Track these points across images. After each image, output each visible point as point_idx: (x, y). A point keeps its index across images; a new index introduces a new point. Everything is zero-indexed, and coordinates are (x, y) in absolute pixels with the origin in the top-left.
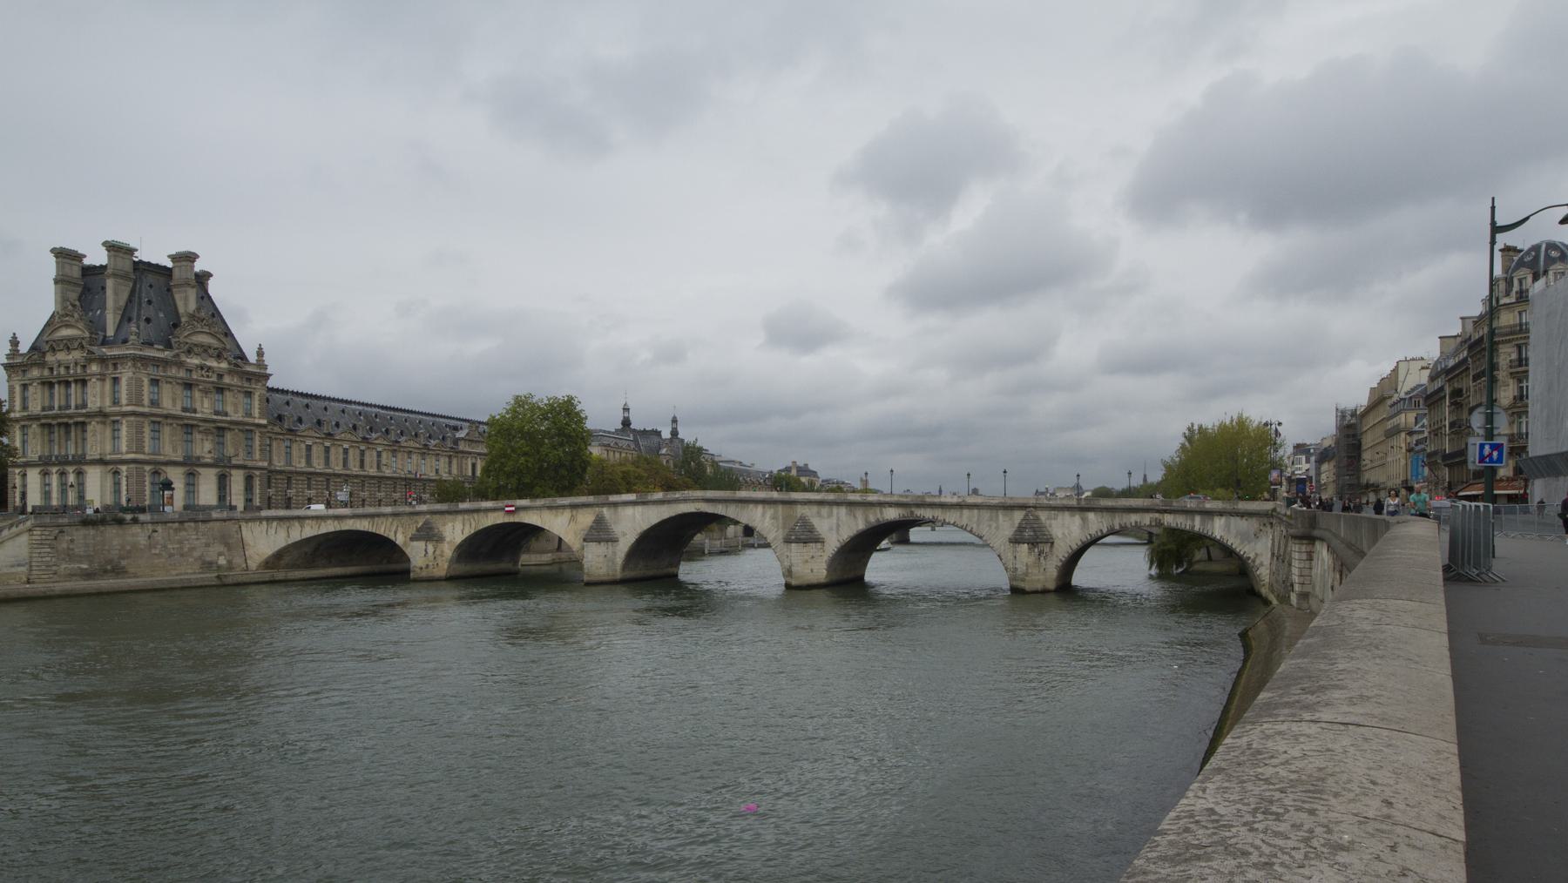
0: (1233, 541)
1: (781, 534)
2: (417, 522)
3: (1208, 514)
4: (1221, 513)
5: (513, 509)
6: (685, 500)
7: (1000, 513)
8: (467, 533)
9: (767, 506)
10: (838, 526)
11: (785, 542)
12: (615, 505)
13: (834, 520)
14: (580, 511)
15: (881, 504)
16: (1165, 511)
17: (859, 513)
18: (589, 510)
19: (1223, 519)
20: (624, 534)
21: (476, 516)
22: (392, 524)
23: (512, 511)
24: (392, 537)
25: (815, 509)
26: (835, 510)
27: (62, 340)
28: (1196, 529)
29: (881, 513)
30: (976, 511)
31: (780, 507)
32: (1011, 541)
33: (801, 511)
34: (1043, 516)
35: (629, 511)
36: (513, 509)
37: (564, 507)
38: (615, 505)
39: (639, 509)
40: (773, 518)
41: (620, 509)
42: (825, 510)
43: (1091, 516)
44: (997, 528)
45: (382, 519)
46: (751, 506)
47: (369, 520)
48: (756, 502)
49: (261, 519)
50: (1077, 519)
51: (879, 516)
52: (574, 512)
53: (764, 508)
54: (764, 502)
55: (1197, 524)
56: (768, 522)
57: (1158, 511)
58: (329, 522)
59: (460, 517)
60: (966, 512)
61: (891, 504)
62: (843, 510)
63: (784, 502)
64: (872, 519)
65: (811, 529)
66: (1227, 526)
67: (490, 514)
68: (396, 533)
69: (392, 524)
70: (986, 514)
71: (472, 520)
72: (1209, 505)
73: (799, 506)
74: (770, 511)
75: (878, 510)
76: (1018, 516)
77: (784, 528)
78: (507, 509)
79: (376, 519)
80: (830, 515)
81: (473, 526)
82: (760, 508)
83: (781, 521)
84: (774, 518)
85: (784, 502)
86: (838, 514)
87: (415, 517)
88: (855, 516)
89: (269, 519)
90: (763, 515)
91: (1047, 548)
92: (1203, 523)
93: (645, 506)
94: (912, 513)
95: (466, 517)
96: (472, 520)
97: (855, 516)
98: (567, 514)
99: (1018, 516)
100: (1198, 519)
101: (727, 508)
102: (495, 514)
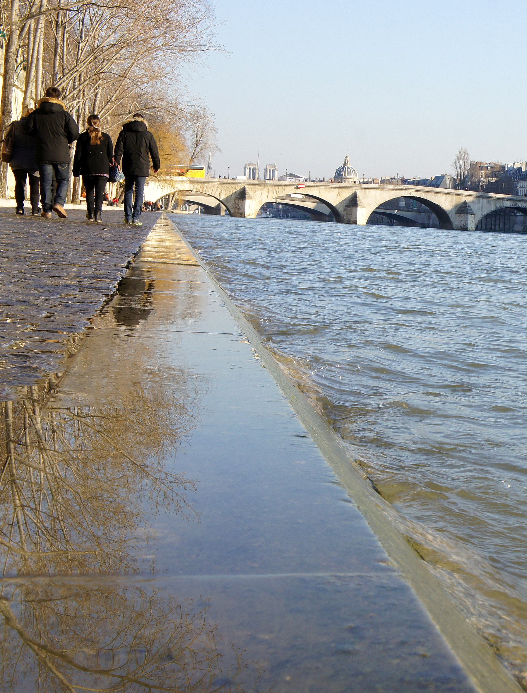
5: (304, 186)
6: (405, 189)
9: (447, 196)
10: (482, 208)
11: (456, 214)
12: (365, 188)
13: (481, 205)
14: (344, 190)
21: (277, 188)
23: (304, 188)
29: (503, 203)
31: (455, 196)
35: (373, 192)
36: (304, 186)
37: (335, 187)
38: (365, 188)
39: (379, 192)
40: (451, 202)
41: (368, 191)
46: (440, 195)
48: (443, 193)
51: (501, 204)
52: (340, 190)
53: (446, 196)
54: (447, 194)
59: (266, 188)
63: (457, 195)
64: (498, 206)
67: (286, 188)
71: (274, 191)
73: (464, 197)
74: (449, 198)
78: (299, 186)
79: (206, 185)
81: (275, 193)
85: (457, 195)
86: (482, 202)
88: (490, 204)
90: (445, 200)
94: (516, 204)
97: (490, 204)
98: (336, 191)
101: (427, 194)
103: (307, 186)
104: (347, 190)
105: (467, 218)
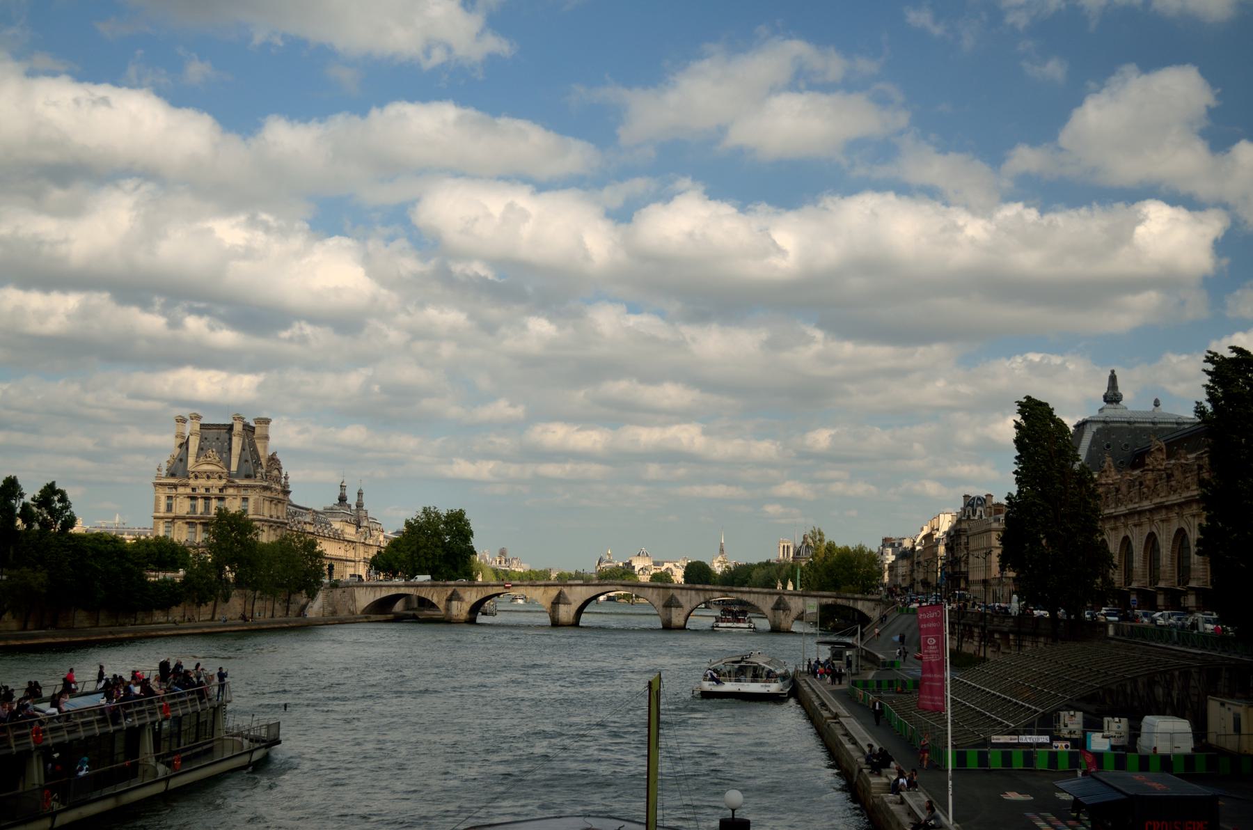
0: (865, 611)
1: (661, 603)
2: (446, 590)
3: (856, 600)
4: (861, 599)
7: (768, 596)
8: (478, 599)
10: (691, 600)
12: (571, 585)
13: (689, 598)
14: (550, 587)
16: (838, 598)
17: (701, 594)
18: (555, 587)
20: (575, 601)
21: (485, 588)
22: (430, 591)
24: (430, 598)
25: (679, 591)
26: (689, 592)
27: (206, 472)
30: (756, 595)
31: (661, 590)
32: (772, 609)
33: (671, 592)
34: (786, 598)
35: (579, 588)
37: (541, 585)
38: (571, 585)
39: (584, 588)
41: (573, 588)
42: (684, 592)
44: (766, 603)
45: (423, 588)
46: (646, 589)
47: (415, 588)
52: (546, 588)
55: (851, 603)
56: (655, 597)
57: (835, 598)
58: (393, 588)
59: (475, 589)
60: (752, 595)
62: (693, 592)
63: (663, 588)
65: (678, 602)
66: (863, 605)
67: (494, 588)
68: (432, 596)
69: (430, 591)
70: (761, 596)
72: (856, 596)
73: (671, 590)
74: (656, 591)
75: (711, 593)
76: (776, 598)
77: (663, 600)
79: (419, 588)
80: (687, 594)
81: (484, 593)
82: (651, 590)
83: (661, 596)
84: (658, 595)
85: (663, 588)
87: (446, 588)
90: (652, 594)
91: (788, 612)
92: (853, 603)
93: (588, 587)
99: (776, 598)
100: (851, 601)
102: (498, 588)
103: (513, 586)
104: (553, 587)
105: (671, 611)
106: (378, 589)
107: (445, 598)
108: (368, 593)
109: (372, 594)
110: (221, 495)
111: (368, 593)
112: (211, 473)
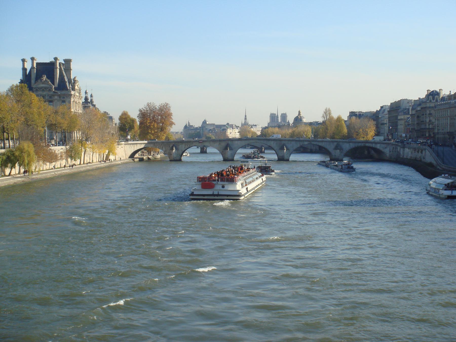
0: (381, 149)
15: (303, 141)
19: (379, 145)
26: (292, 142)
28: (373, 146)
34: (341, 144)
35: (236, 142)
43: (351, 144)
49: (128, 144)
50: (348, 145)
57: (365, 143)
59: (184, 144)
61: (306, 141)
62: (294, 142)
71: (188, 145)
76: (335, 144)
81: (188, 146)
89: (130, 144)
95: (186, 144)
96: (188, 145)
100: (374, 144)
106: (135, 145)
107: (169, 148)
108: (131, 147)
109: (133, 147)
110: (50, 99)
111: (131, 147)
112: (45, 88)
